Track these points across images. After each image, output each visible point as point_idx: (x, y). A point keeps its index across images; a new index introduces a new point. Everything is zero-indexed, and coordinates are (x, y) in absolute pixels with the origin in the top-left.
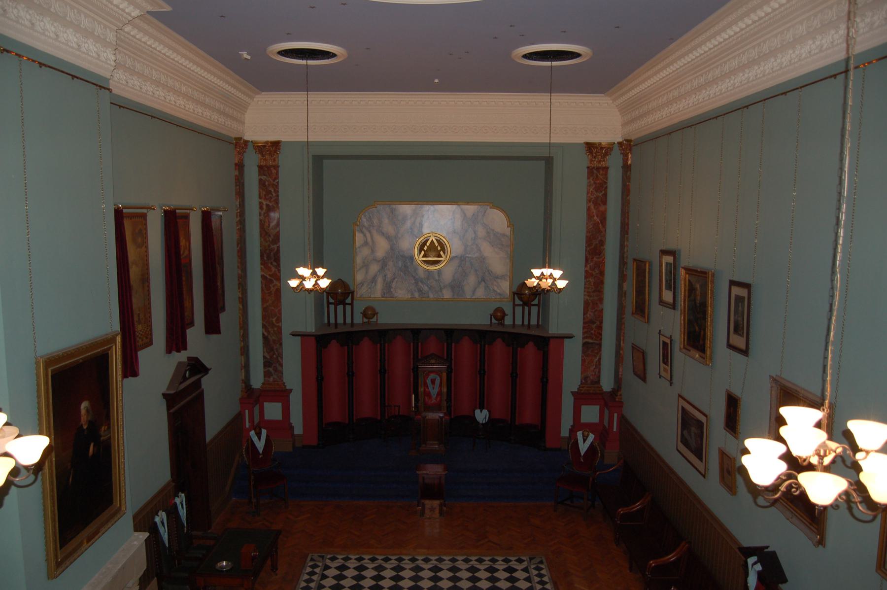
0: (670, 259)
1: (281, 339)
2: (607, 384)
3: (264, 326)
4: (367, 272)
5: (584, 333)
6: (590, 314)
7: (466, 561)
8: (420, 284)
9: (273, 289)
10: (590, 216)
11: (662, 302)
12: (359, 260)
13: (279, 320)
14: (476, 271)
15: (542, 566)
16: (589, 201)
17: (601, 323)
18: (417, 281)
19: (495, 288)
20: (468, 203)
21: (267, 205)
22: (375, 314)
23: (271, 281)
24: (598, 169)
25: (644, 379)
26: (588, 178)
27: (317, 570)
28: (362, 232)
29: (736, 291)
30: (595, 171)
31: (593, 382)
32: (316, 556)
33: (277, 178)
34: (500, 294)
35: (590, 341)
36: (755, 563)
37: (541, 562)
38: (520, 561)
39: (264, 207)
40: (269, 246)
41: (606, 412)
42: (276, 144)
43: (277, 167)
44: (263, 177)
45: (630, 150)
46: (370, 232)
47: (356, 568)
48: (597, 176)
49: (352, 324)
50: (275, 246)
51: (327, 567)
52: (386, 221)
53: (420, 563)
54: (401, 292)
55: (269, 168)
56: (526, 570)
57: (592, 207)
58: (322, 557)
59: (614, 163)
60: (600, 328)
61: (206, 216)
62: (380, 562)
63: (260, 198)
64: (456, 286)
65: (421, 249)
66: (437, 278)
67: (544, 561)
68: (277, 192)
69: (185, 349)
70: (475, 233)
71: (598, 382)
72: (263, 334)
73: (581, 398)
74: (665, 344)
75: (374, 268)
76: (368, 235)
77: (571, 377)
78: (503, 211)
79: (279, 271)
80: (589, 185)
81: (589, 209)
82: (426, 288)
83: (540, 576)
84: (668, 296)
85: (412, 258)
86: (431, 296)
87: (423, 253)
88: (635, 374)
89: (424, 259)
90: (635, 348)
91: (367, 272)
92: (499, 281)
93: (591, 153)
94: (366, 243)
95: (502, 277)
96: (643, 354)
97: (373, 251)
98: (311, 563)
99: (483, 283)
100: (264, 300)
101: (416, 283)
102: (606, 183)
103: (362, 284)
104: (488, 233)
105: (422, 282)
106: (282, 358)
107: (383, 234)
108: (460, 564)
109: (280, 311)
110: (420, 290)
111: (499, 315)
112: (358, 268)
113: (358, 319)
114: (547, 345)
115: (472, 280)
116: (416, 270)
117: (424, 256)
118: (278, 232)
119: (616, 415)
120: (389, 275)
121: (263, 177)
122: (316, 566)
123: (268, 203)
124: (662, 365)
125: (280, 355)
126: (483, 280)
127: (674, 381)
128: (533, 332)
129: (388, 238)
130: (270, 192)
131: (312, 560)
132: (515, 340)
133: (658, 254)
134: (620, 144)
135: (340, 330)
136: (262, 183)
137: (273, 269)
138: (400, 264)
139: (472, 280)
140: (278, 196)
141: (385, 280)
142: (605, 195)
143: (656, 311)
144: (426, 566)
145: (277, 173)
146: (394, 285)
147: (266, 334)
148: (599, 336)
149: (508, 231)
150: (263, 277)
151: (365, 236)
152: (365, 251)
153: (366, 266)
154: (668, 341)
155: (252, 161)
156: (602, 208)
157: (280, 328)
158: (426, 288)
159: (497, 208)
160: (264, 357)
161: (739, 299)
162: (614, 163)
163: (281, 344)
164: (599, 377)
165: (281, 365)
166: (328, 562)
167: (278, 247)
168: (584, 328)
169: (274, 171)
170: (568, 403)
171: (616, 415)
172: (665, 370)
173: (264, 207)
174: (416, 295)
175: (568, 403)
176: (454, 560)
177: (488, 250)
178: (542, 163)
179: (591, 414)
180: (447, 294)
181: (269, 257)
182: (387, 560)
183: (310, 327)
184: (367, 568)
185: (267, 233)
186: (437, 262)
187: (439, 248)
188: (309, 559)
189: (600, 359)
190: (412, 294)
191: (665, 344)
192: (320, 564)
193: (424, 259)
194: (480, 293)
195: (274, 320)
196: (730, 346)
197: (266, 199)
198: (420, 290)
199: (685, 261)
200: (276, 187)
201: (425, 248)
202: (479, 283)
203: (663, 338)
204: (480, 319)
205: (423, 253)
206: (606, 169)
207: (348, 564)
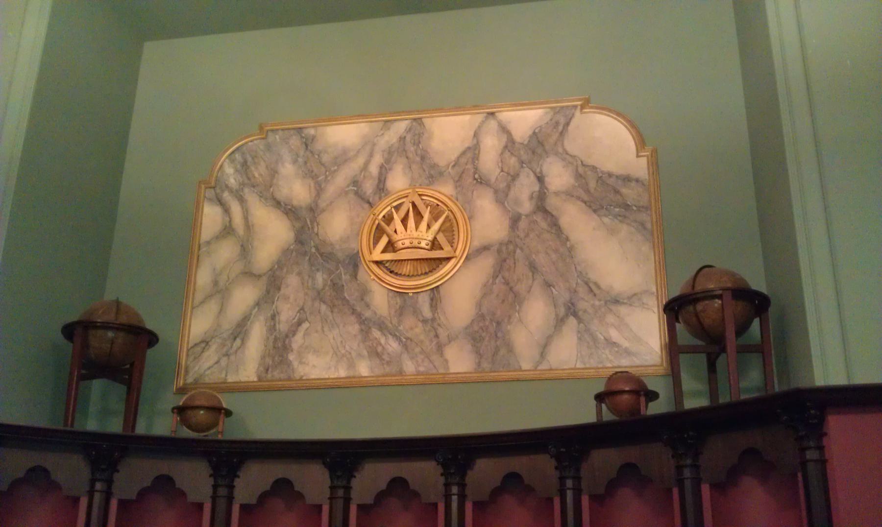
4: (221, 311)
8: (376, 333)
12: (203, 278)
14: (548, 285)
19: (614, 335)
20: (518, 104)
28: (220, 202)
46: (242, 200)
52: (288, 169)
66: (427, 313)
70: (540, 179)
75: (244, 296)
76: (236, 209)
82: (393, 346)
86: (409, 367)
87: (384, 241)
89: (388, 256)
91: (221, 311)
92: (623, 310)
94: (228, 230)
95: (632, 299)
97: (245, 251)
99: (572, 321)
101: (365, 333)
103: (205, 343)
104: (579, 176)
105: (382, 326)
107: (278, 204)
112: (199, 297)
116: (364, 292)
117: (391, 246)
120: (287, 313)
126: (572, 310)
129: (289, 210)
138: (320, 278)
141: (272, 329)
146: (298, 340)
149: (640, 167)
151: (227, 210)
152: (226, 252)
153: (220, 291)
180: (459, 361)
193: (388, 256)
194: (566, 353)
202: (560, 322)
205: (384, 241)
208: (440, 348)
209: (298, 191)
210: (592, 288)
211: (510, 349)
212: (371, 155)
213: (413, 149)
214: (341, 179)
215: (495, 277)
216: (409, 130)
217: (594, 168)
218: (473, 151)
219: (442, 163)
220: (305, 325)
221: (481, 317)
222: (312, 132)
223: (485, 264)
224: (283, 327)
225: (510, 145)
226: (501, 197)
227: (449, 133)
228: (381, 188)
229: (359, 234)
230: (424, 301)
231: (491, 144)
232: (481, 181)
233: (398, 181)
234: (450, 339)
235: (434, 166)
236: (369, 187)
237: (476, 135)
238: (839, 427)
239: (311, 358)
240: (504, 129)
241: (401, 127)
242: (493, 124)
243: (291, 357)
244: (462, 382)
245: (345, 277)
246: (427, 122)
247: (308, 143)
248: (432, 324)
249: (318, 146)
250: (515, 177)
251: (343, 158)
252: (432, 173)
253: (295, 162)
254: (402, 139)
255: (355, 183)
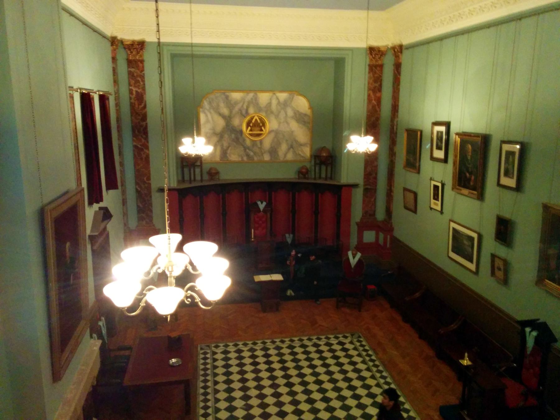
0: (443, 129)
1: (150, 192)
2: (380, 215)
3: (137, 183)
5: (365, 182)
6: (369, 169)
7: (310, 340)
8: (248, 150)
9: (144, 156)
10: (369, 100)
11: (433, 158)
13: (149, 178)
14: (287, 141)
15: (362, 339)
16: (369, 89)
17: (376, 174)
18: (245, 148)
19: (300, 153)
20: (282, 91)
21: (136, 91)
22: (217, 173)
23: (142, 150)
24: (376, 66)
25: (415, 211)
26: (369, 73)
27: (208, 356)
28: (205, 113)
29: (506, 147)
30: (374, 68)
31: (370, 215)
32: (203, 346)
33: (143, 70)
34: (303, 157)
35: (369, 187)
36: (530, 332)
37: (360, 337)
38: (346, 337)
39: (134, 93)
40: (139, 123)
41: (381, 236)
42: (141, 45)
43: (142, 61)
44: (132, 70)
45: (401, 52)
46: (210, 113)
47: (235, 352)
48: (375, 70)
49: (202, 180)
50: (144, 123)
51: (214, 353)
52: (222, 105)
53: (278, 344)
54: (234, 157)
55: (136, 61)
56: (351, 343)
57: (372, 94)
58: (208, 346)
59: (388, 62)
60: (375, 178)
61: (103, 99)
62: (250, 346)
63: (130, 85)
64: (273, 151)
65: (248, 125)
67: (361, 335)
68: (143, 81)
69: (101, 200)
71: (374, 214)
72: (137, 190)
73: (363, 226)
74: (436, 187)
77: (357, 212)
78: (305, 97)
79: (148, 142)
80: (370, 78)
81: (369, 95)
83: (362, 346)
84: (440, 154)
85: (241, 132)
86: (256, 159)
87: (249, 128)
88: (406, 208)
89: (251, 132)
90: (405, 190)
93: (371, 55)
95: (304, 145)
96: (415, 195)
98: (202, 351)
99: (292, 149)
100: (136, 164)
101: (245, 150)
102: (381, 76)
104: (295, 113)
106: (152, 206)
108: (306, 342)
109: (149, 171)
110: (248, 155)
111: (303, 172)
113: (206, 177)
114: (340, 192)
115: (284, 147)
116: (244, 140)
117: (251, 130)
118: (146, 112)
119: (389, 237)
120: (225, 144)
121: (132, 70)
122: (205, 353)
123: (137, 89)
124: (433, 201)
125: (151, 204)
127: (443, 211)
128: (328, 182)
129: (223, 117)
130: (138, 82)
131: (202, 349)
132: (317, 189)
133: (430, 125)
134: (393, 48)
135: (193, 185)
136: (130, 74)
137: (143, 140)
138: (233, 136)
139: (284, 147)
140: (144, 84)
142: (381, 86)
143: (426, 164)
144: (284, 346)
145: (143, 67)
146: (229, 152)
147: (139, 189)
148: (375, 183)
149: (309, 112)
150: (135, 147)
151: (207, 116)
154: (439, 185)
155: (122, 56)
156: (378, 95)
157: (150, 184)
158: (252, 154)
159: (301, 95)
160: (138, 206)
161: (510, 154)
162: (388, 62)
163: (151, 197)
164: (375, 211)
165: (151, 211)
166: (214, 349)
167: (147, 124)
168: (365, 178)
169: (140, 65)
170: (354, 229)
171: (389, 237)
172: (435, 204)
173: (134, 93)
174: (245, 159)
175: (354, 229)
176: (301, 340)
177: (294, 126)
178: (332, 63)
179: (369, 236)
180: (267, 157)
181: (139, 131)
182: (255, 344)
183: (174, 184)
184: (243, 351)
185: (137, 113)
186: (259, 135)
187: (261, 125)
188: (199, 348)
189: (375, 199)
190: (242, 158)
191: (436, 187)
192: (209, 351)
193: (251, 132)
195: (145, 179)
196: (499, 184)
197: (135, 87)
198: (248, 155)
199: (454, 128)
200: (143, 77)
201: (251, 125)
202: (289, 149)
203: (433, 183)
204: (288, 174)
205: (249, 128)
206: (381, 66)
207: (228, 349)
208: (262, 154)
209: (225, 111)
210: (296, 141)
211: (278, 155)
212: (244, 103)
213: (255, 102)
214: (236, 109)
215: (275, 137)
216: (253, 96)
217: (298, 111)
218: (269, 104)
219: (262, 106)
220: (230, 148)
221: (272, 147)
222: (228, 94)
223: (272, 135)
224: (225, 148)
225: (279, 103)
226: (277, 117)
227: (264, 98)
228: (247, 113)
229: (241, 125)
230: (258, 143)
231: (274, 102)
232: (272, 112)
233: (251, 111)
234: (265, 152)
235: (260, 107)
236: (244, 112)
237: (271, 99)
238: (344, 188)
239: (232, 156)
240: (277, 98)
241: (251, 95)
242: (275, 97)
243: (228, 155)
244: (266, 162)
245: (239, 136)
246: (258, 94)
247: (227, 97)
248: (260, 148)
249: (230, 99)
250: (280, 112)
251: (236, 103)
252: (259, 109)
253: (224, 103)
254: (252, 99)
255: (240, 110)
